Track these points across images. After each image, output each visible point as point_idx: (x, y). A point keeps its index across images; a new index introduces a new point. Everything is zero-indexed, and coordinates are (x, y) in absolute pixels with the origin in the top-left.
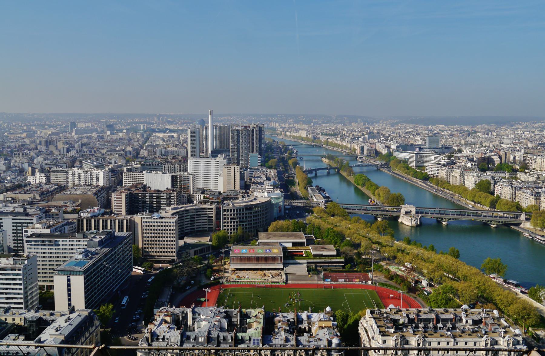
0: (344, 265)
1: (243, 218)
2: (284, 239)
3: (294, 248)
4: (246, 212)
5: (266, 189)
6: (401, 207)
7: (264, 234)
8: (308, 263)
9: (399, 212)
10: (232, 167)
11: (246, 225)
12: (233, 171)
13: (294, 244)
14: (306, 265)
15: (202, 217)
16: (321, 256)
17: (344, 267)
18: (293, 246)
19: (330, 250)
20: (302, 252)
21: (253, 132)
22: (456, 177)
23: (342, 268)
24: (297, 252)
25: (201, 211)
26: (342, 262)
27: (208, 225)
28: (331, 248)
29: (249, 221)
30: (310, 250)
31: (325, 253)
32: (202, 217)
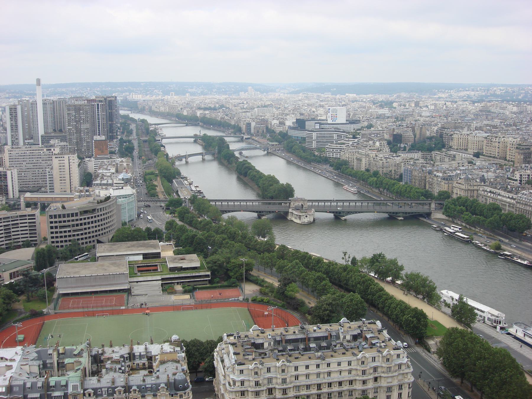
0: (210, 279)
1: (77, 225)
2: (132, 250)
3: (147, 261)
4: (81, 217)
5: (114, 185)
6: (290, 200)
7: (106, 246)
8: (163, 279)
9: (289, 207)
10: (65, 156)
11: (82, 234)
12: (66, 162)
13: (146, 256)
14: (160, 282)
15: (21, 227)
16: (181, 269)
17: (210, 282)
18: (144, 258)
19: (192, 261)
20: (156, 265)
21: (98, 108)
22: (361, 160)
23: (207, 282)
24: (150, 266)
25: (19, 218)
26: (207, 276)
27: (30, 237)
28: (193, 259)
29: (85, 229)
30: (166, 262)
31: (184, 266)
32: (21, 227)
